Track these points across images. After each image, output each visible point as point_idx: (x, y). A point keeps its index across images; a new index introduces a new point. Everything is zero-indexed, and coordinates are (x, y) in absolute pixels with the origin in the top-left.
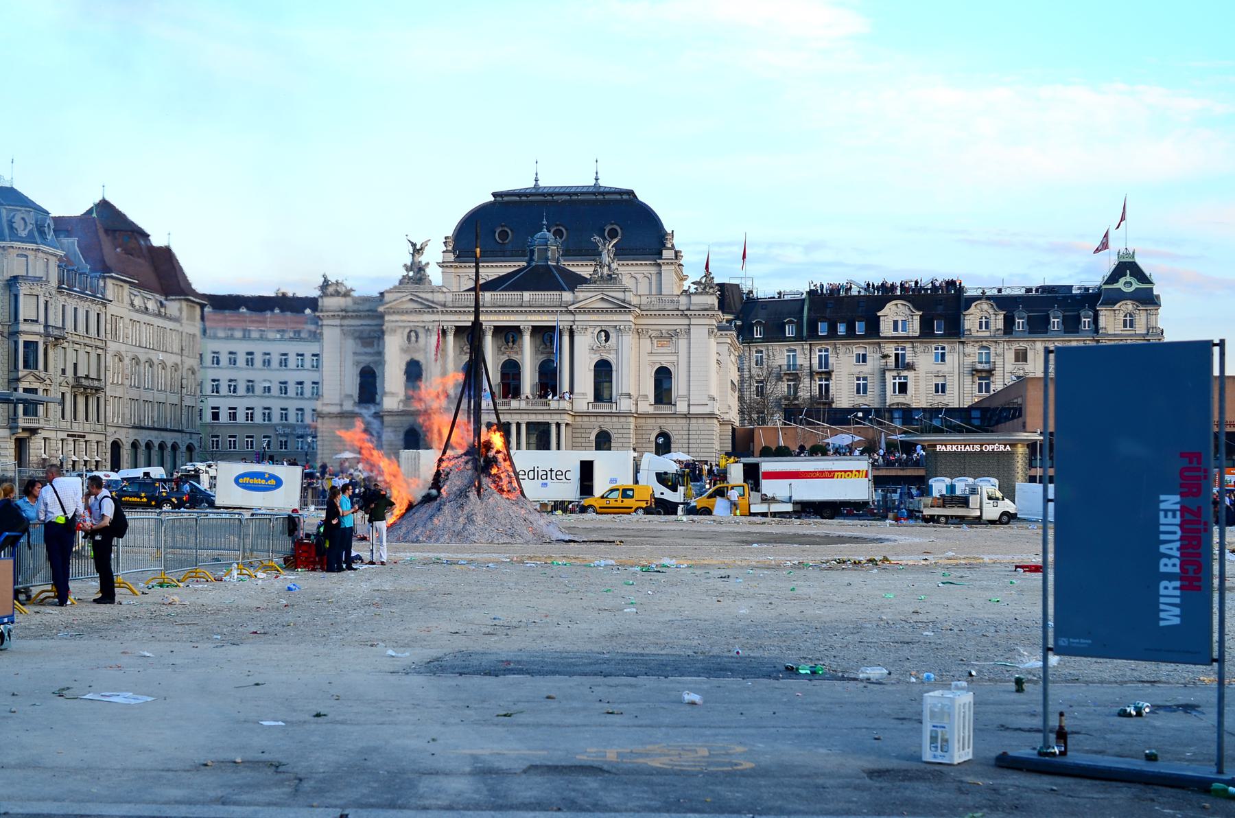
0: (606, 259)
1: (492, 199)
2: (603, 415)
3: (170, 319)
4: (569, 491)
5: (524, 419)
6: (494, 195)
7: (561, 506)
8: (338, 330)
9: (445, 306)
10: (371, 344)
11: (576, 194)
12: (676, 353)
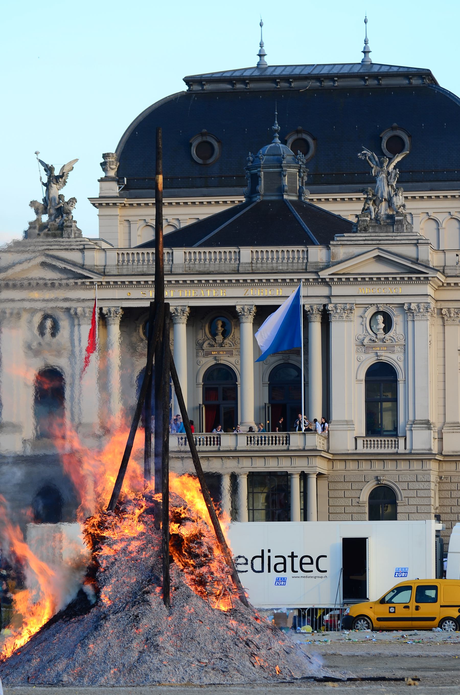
0: (385, 190)
1: (185, 88)
2: (382, 458)
4: (323, 591)
5: (245, 467)
6: (188, 81)
7: (312, 617)
9: (104, 274)
11: (330, 77)
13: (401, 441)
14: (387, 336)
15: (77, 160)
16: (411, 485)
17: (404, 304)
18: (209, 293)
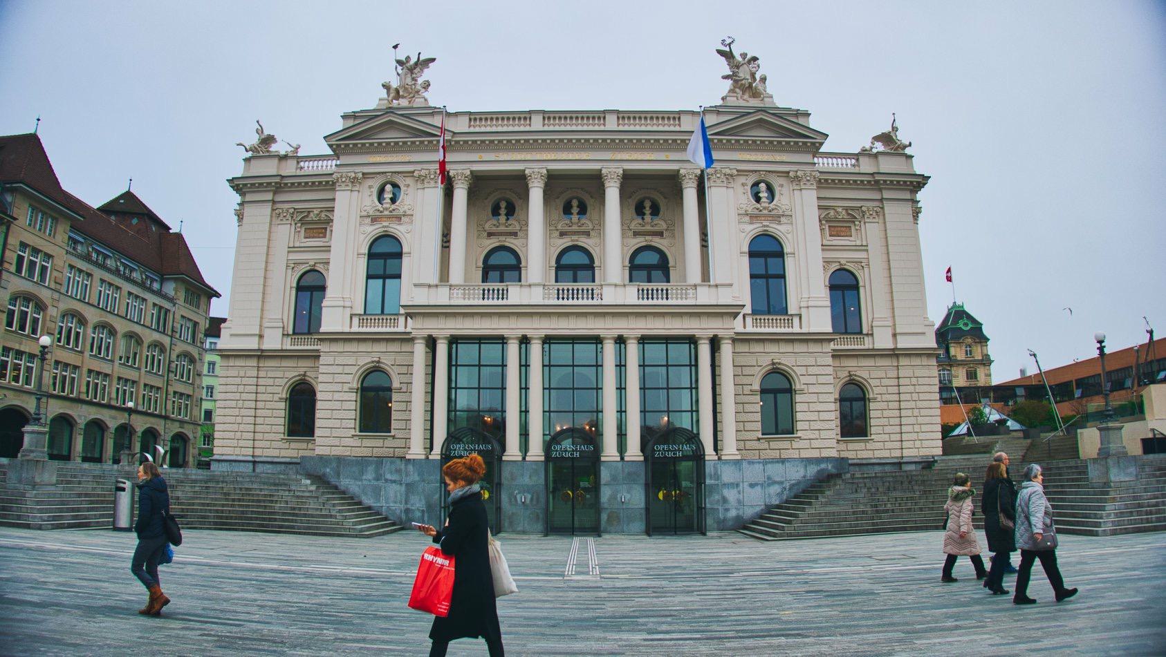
3: (165, 297)
8: (267, 209)
12: (864, 248)
13: (796, 320)
14: (772, 206)
15: (434, 60)
16: (811, 370)
18: (571, 156)
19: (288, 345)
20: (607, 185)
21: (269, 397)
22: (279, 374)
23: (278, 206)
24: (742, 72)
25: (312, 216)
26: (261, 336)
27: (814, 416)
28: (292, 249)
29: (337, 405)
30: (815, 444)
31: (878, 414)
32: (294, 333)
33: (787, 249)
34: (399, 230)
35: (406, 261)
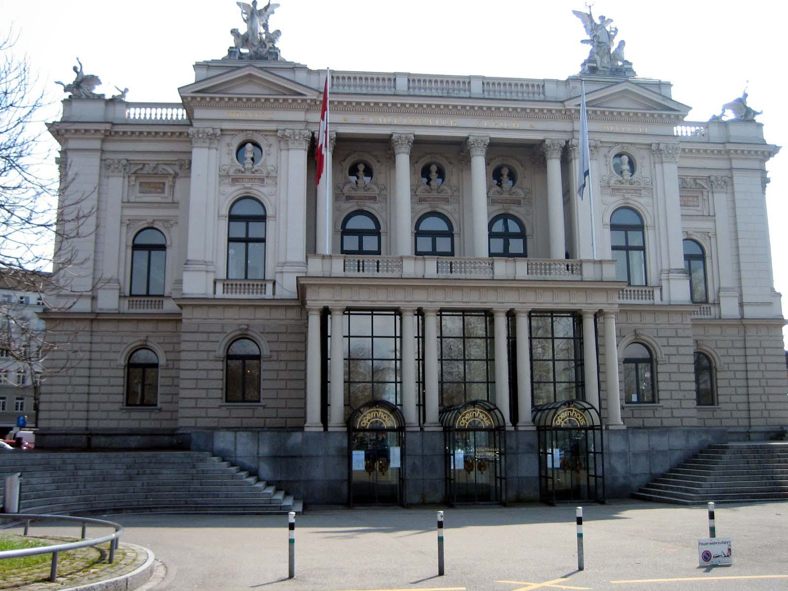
8: (94, 161)
10: (160, 188)
12: (712, 217)
16: (672, 341)
17: (651, 145)
19: (125, 306)
20: (473, 152)
21: (106, 364)
22: (119, 340)
23: (107, 156)
24: (599, 35)
25: (147, 170)
26: (94, 298)
27: (674, 386)
28: (127, 203)
29: (203, 374)
30: (676, 413)
31: (725, 383)
32: (131, 295)
33: (648, 221)
34: (262, 191)
35: (270, 223)
